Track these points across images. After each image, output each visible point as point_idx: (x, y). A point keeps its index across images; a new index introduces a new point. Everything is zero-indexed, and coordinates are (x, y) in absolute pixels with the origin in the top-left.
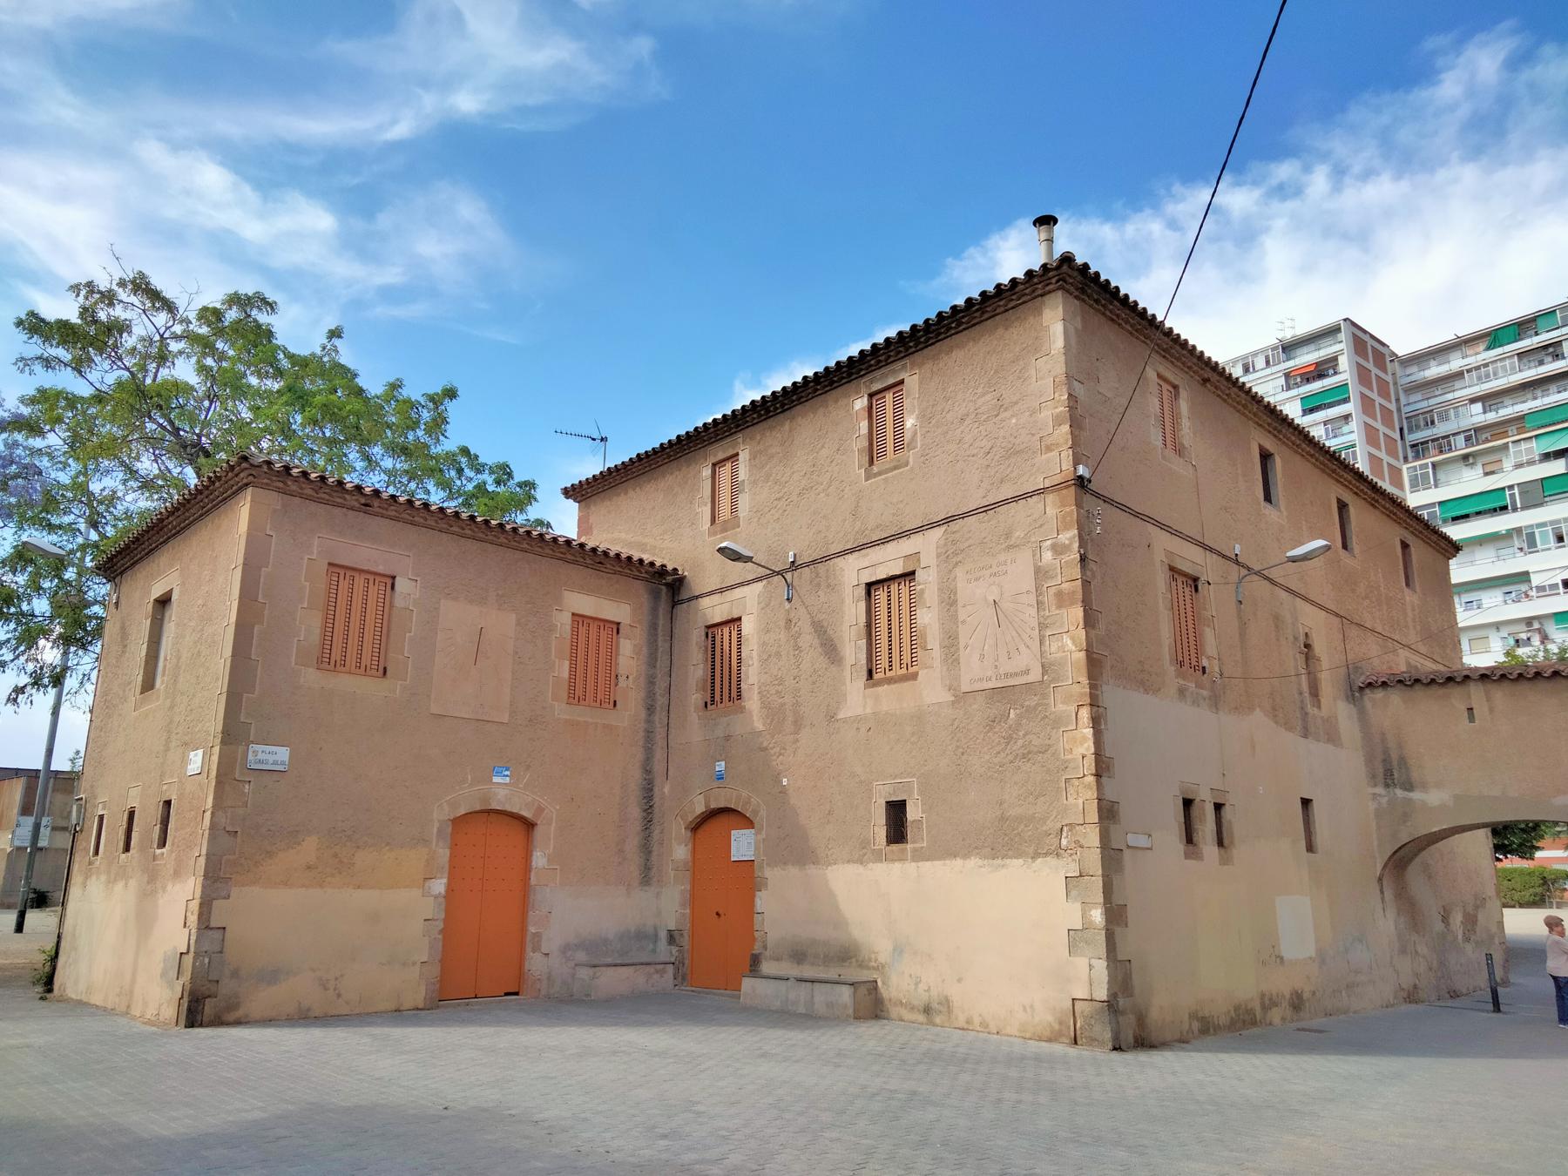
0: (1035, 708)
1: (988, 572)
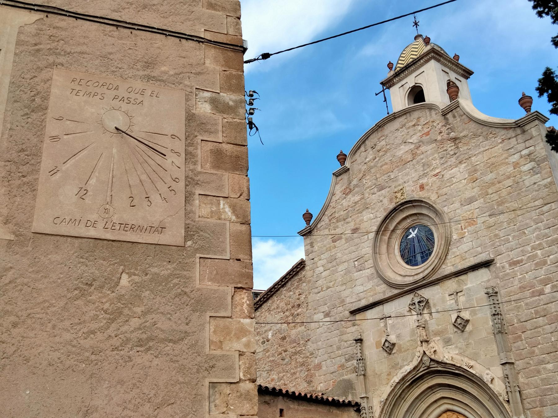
0: (167, 279)
1: (114, 93)
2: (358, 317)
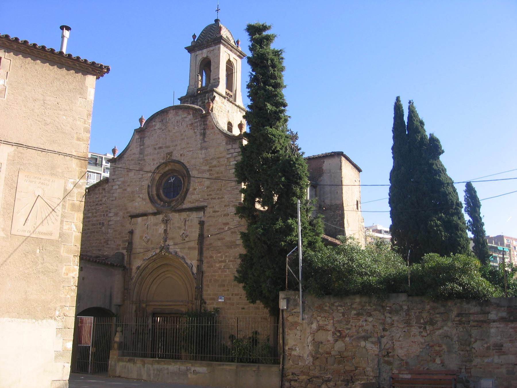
2: (134, 220)
